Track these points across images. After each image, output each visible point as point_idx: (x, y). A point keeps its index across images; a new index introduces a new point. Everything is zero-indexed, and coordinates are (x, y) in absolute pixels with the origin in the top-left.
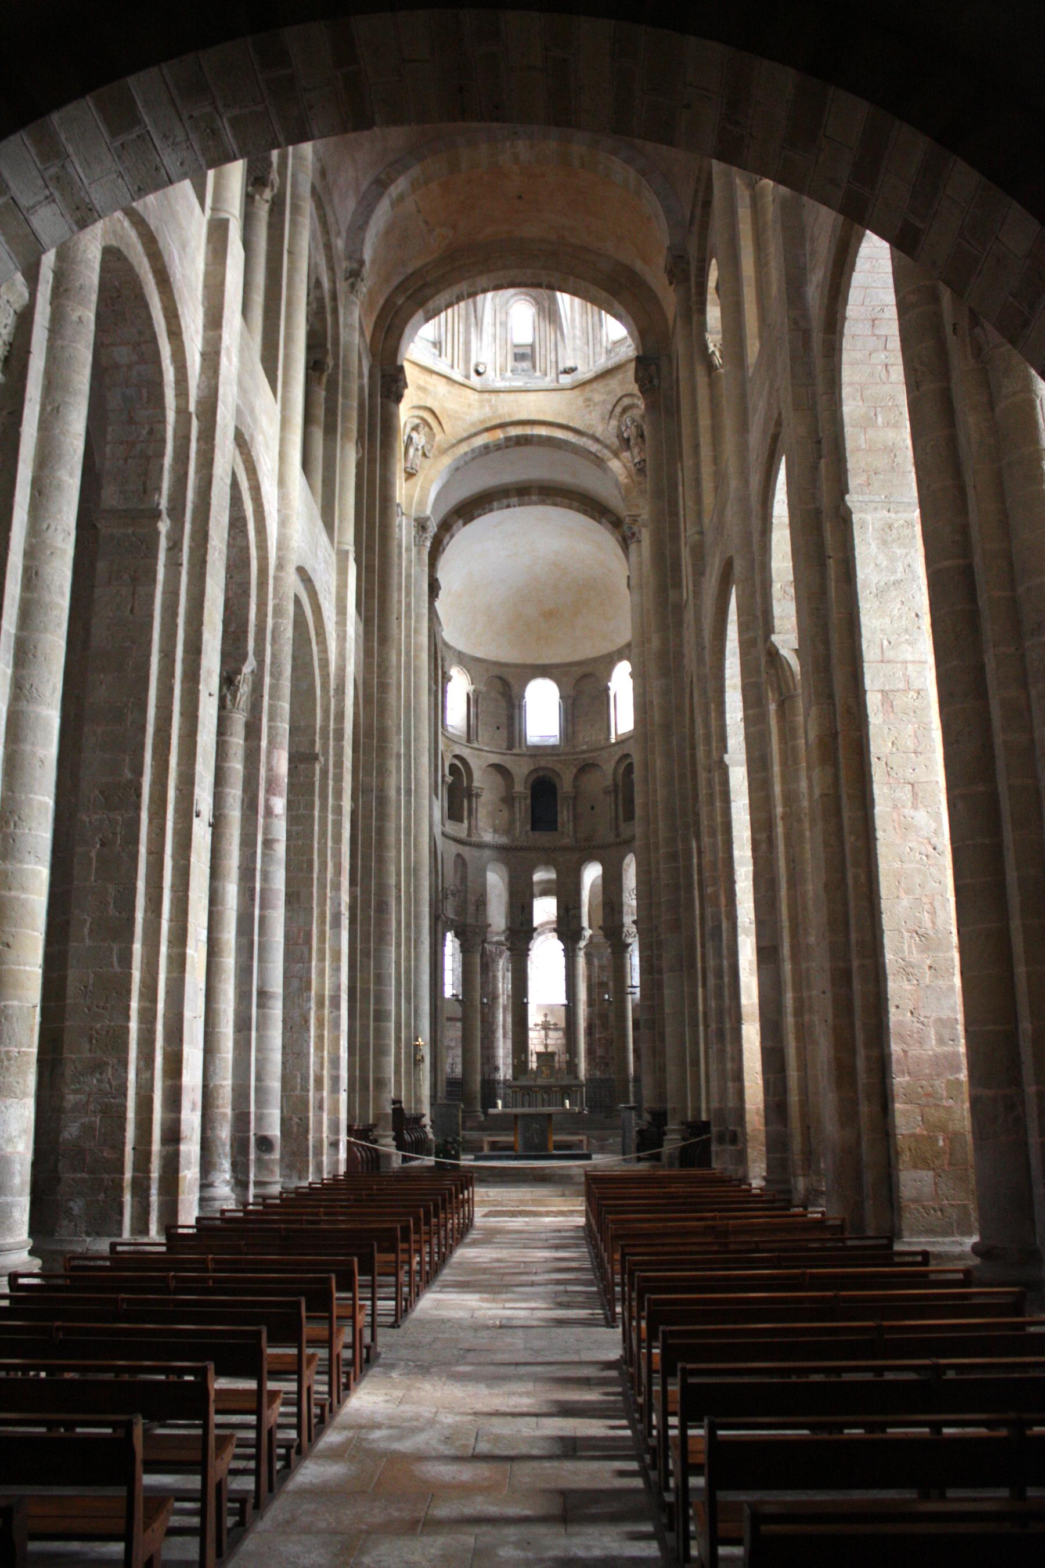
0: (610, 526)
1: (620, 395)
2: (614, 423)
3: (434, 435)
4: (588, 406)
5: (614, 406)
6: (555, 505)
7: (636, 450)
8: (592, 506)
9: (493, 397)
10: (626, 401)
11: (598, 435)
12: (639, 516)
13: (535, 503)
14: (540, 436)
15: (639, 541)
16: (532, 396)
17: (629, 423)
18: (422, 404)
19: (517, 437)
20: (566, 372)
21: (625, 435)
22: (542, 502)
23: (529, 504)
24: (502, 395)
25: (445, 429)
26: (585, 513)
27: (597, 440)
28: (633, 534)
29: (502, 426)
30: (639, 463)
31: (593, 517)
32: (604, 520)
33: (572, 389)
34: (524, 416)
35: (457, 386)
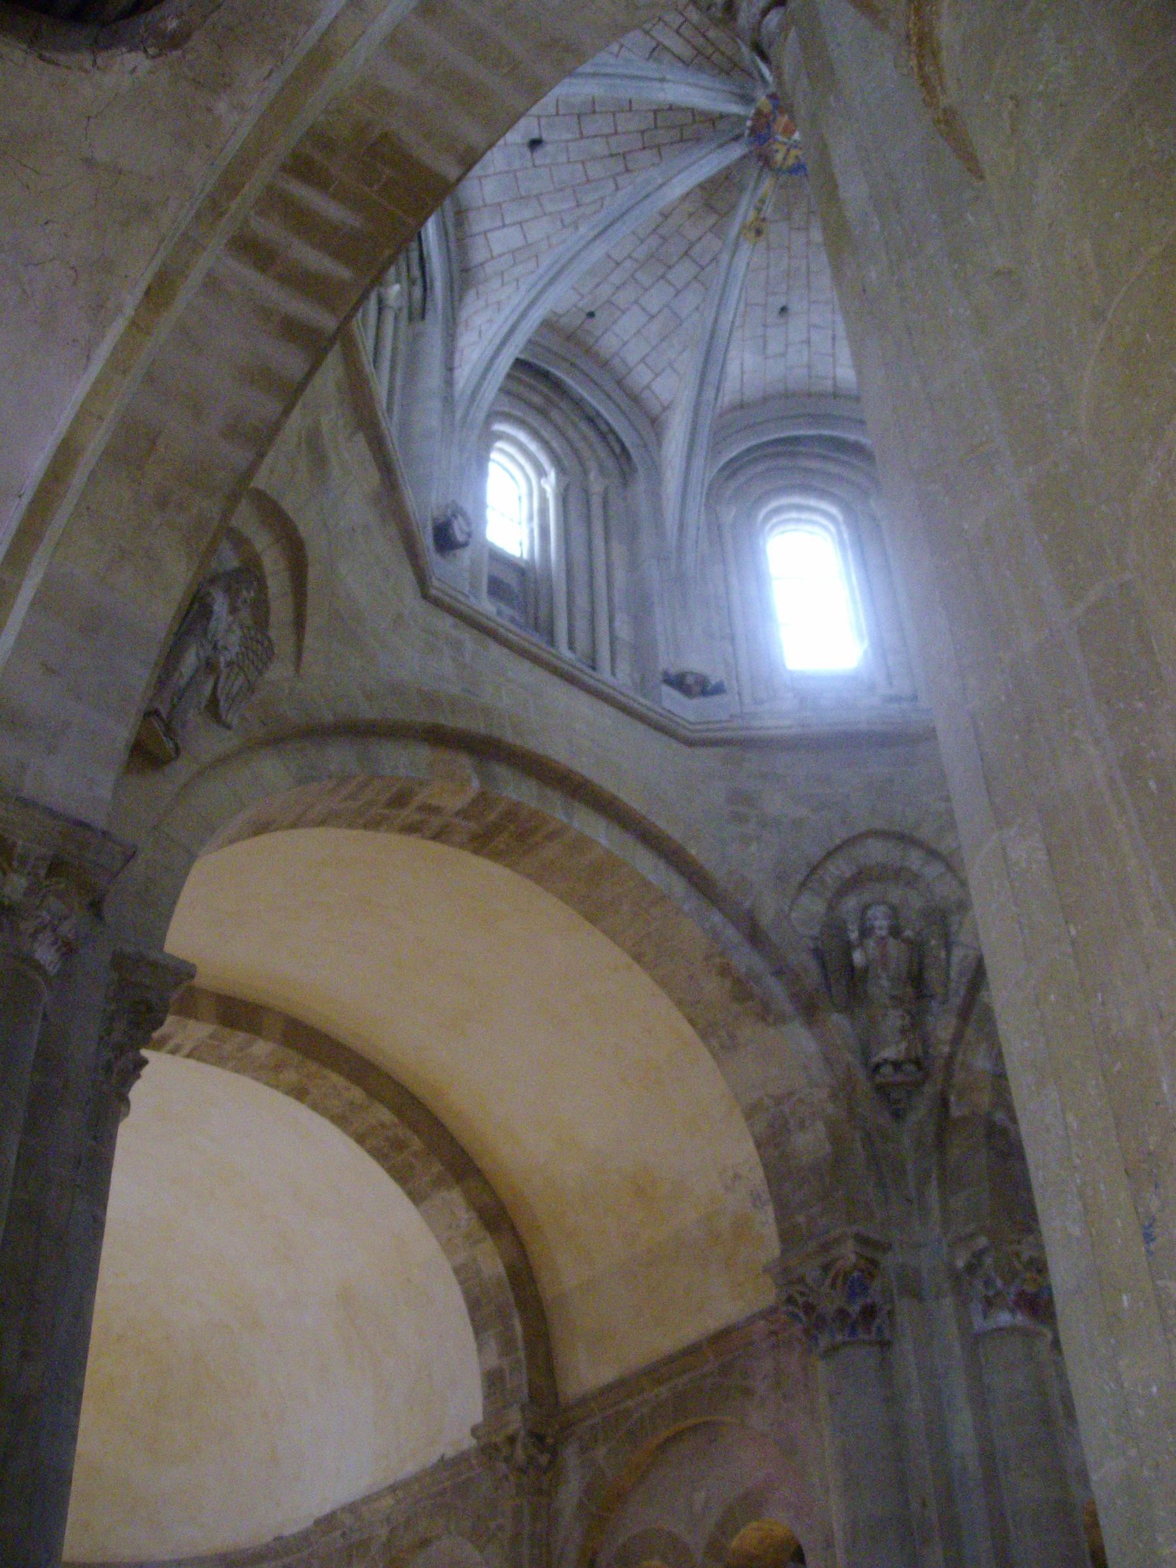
0: (465, 1216)
1: (862, 827)
2: (813, 905)
3: (269, 653)
4: (739, 818)
5: (829, 854)
6: (299, 1093)
7: (894, 1020)
8: (421, 1140)
9: (467, 637)
10: (877, 852)
11: (766, 920)
12: (886, 1248)
13: (243, 1065)
14: (582, 844)
15: (885, 1345)
16: (583, 704)
17: (881, 923)
18: (288, 504)
19: (512, 813)
20: (679, 682)
21: (858, 957)
22: (268, 1073)
23: (221, 1061)
24: (495, 650)
25: (307, 657)
26: (388, 1153)
27: (755, 936)
28: (869, 1312)
29: (486, 749)
30: (897, 1065)
31: (401, 1176)
32: (454, 1196)
33: (690, 743)
34: (557, 751)
35: (392, 529)
